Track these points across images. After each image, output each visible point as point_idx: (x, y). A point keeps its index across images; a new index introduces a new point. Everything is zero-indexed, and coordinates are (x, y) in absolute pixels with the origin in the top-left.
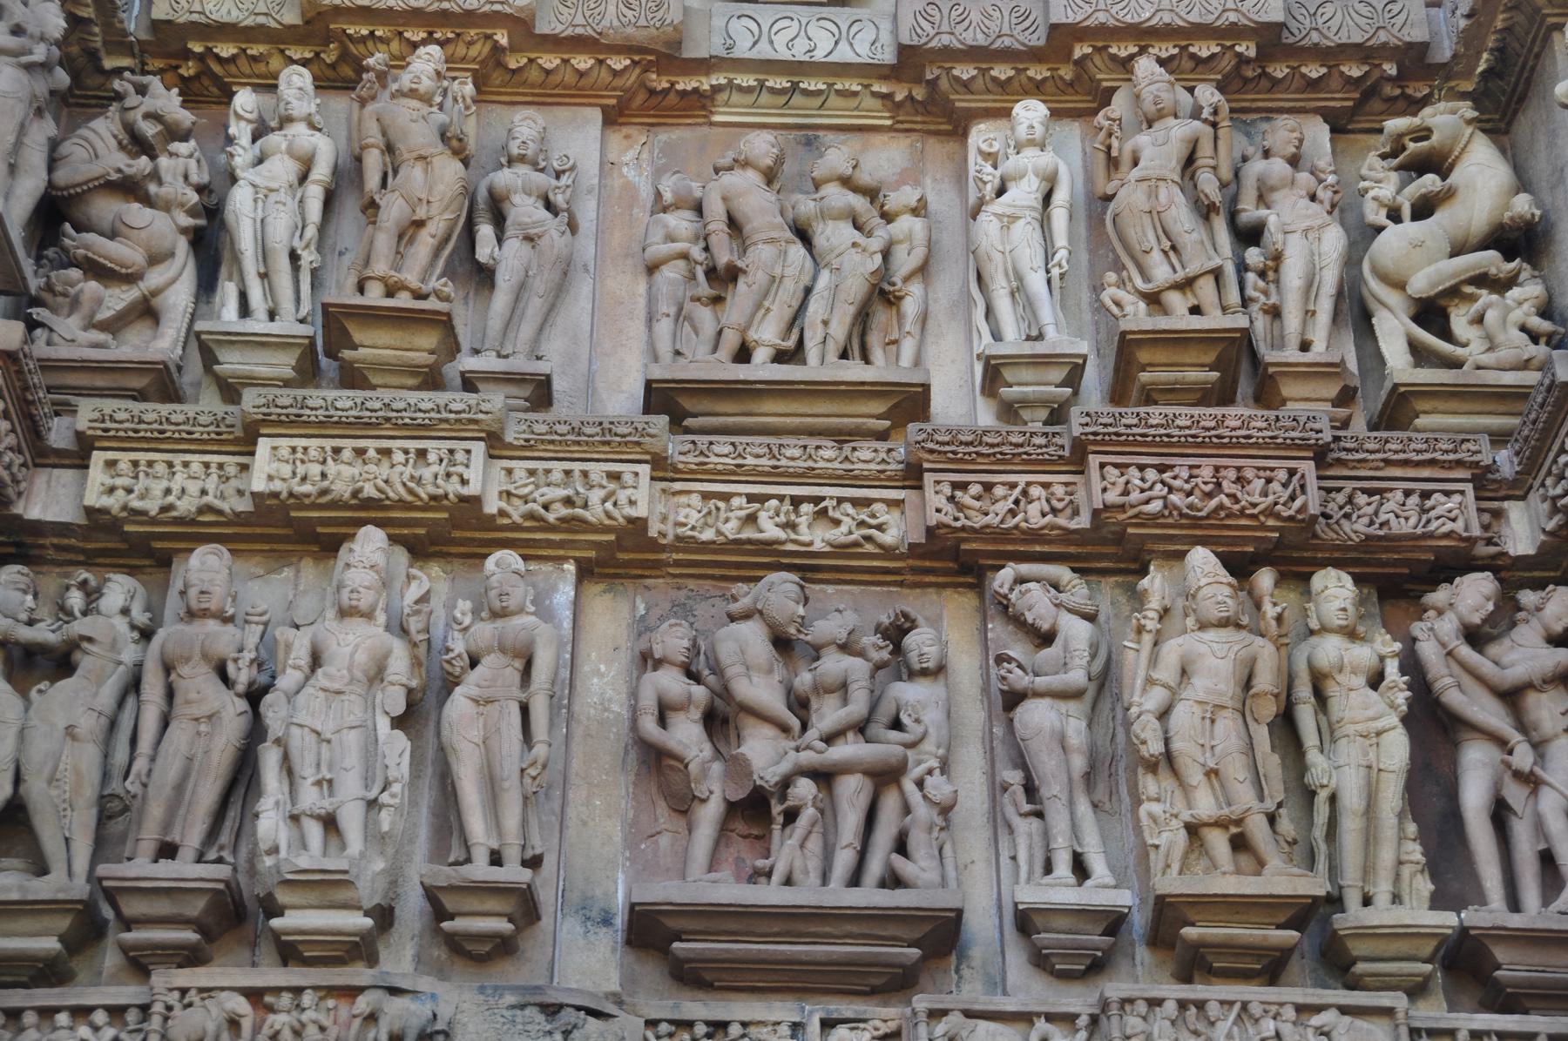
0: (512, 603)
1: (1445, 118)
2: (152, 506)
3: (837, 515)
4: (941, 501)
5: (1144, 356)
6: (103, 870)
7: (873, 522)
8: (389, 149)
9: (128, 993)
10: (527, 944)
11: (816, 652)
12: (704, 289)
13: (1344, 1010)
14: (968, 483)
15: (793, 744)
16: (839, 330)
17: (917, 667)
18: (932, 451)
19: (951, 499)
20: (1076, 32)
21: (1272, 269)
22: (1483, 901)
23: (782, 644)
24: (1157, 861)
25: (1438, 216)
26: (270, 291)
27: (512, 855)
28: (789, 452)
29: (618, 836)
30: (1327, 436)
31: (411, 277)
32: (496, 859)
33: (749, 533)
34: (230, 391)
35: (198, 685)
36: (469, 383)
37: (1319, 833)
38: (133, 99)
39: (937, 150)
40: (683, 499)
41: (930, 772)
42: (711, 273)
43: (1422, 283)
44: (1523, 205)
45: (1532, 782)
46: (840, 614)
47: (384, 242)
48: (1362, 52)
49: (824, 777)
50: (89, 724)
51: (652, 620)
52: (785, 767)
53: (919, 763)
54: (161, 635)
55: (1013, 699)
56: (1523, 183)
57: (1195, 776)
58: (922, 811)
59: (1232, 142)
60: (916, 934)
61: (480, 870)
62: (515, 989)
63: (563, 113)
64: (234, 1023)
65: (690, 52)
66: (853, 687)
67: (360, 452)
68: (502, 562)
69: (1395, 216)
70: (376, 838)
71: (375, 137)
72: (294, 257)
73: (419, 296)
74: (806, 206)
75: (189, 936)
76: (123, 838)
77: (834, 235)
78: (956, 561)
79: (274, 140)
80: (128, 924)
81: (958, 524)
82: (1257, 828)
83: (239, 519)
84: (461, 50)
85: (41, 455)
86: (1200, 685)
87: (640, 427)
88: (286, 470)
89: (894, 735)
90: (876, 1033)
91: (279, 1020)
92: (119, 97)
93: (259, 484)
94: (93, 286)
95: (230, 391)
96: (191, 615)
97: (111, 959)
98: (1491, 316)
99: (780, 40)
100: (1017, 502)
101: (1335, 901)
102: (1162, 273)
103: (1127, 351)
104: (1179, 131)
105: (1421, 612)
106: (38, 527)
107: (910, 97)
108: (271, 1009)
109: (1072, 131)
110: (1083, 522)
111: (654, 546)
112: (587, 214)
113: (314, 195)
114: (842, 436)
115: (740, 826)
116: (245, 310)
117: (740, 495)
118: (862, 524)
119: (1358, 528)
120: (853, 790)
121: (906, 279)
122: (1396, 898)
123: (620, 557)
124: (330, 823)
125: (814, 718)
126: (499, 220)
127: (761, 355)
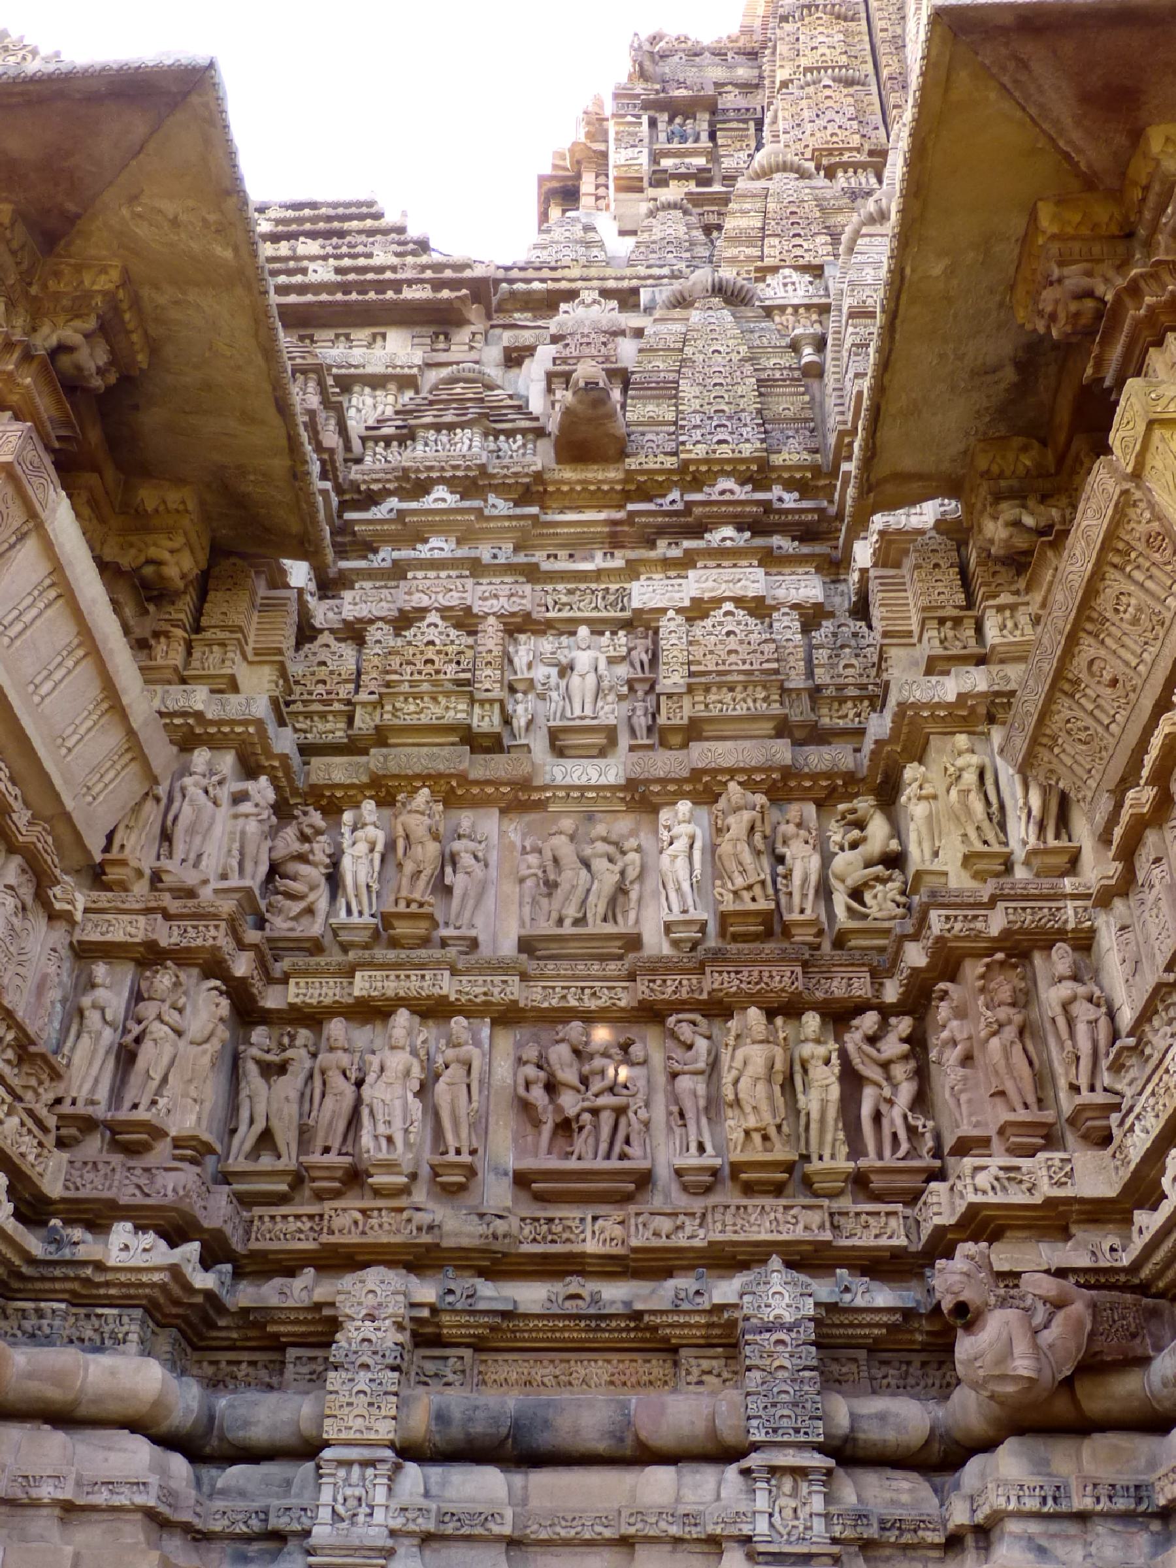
0: (461, 1041)
1: (864, 804)
2: (314, 1001)
4: (644, 988)
5: (731, 920)
6: (302, 1159)
8: (407, 837)
9: (313, 1209)
10: (472, 1185)
11: (591, 1057)
12: (544, 890)
13: (804, 1207)
16: (601, 909)
20: (704, 771)
21: (788, 876)
22: (866, 1155)
23: (577, 1052)
24: (732, 1145)
25: (860, 848)
26: (360, 903)
27: (465, 1150)
29: (510, 1136)
30: (807, 956)
31: (417, 896)
32: (458, 1152)
33: (563, 1004)
34: (345, 948)
35: (336, 1080)
36: (444, 943)
37: (802, 1129)
38: (302, 819)
39: (645, 817)
42: (547, 883)
43: (850, 882)
44: (894, 845)
45: (890, 1102)
47: (405, 882)
48: (828, 775)
49: (595, 1112)
50: (294, 1095)
54: (320, 1057)
55: (674, 1075)
56: (897, 831)
57: (748, 1109)
59: (774, 815)
61: (451, 1157)
62: (466, 1207)
63: (481, 811)
64: (356, 1223)
65: (535, 784)
67: (398, 977)
68: (458, 1023)
69: (842, 849)
70: (408, 1145)
71: (400, 832)
72: (368, 886)
73: (421, 905)
74: (588, 851)
75: (337, 1184)
76: (309, 1142)
77: (600, 864)
78: (651, 1014)
79: (359, 834)
80: (313, 1180)
82: (772, 1131)
83: (348, 1006)
84: (437, 788)
85: (270, 980)
86: (750, 1071)
88: (367, 985)
89: (625, 1092)
91: (374, 1222)
92: (296, 818)
93: (357, 993)
94: (288, 903)
95: (345, 948)
96: (331, 1049)
97: (307, 1193)
98: (880, 895)
99: (575, 776)
101: (806, 1158)
102: (740, 881)
103: (724, 918)
104: (747, 816)
105: (848, 1028)
106: (269, 1011)
107: (633, 798)
108: (370, 1217)
109: (703, 812)
110: (705, 996)
111: (523, 1010)
112: (493, 858)
113: (377, 857)
114: (603, 958)
115: (560, 1132)
116: (349, 912)
119: (820, 995)
120: (607, 1118)
121: (632, 882)
122: (833, 1157)
123: (507, 1016)
124: (390, 1139)
126: (454, 864)
127: (568, 922)
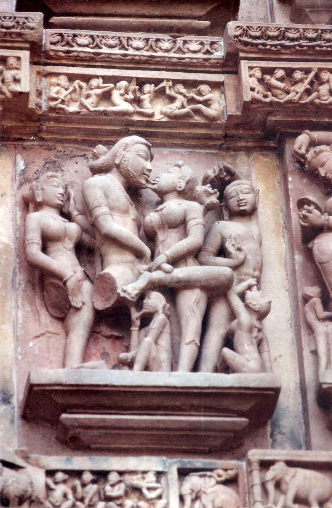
3: (172, 93)
4: (253, 82)
7: (201, 99)
14: (275, 69)
15: (145, 267)
17: (237, 209)
18: (246, 44)
19: (261, 81)
23: (134, 190)
28: (136, 43)
40: (54, 80)
41: (250, 288)
46: (172, 169)
49: (171, 291)
51: (30, 174)
52: (141, 283)
53: (241, 281)
58: (245, 317)
60: (245, 407)
66: (191, 224)
81: (268, 100)
87: (21, 21)
90: (219, 479)
100: (311, 83)
117: (97, 77)
118: (191, 101)
120: (191, 302)
125: (160, 248)
